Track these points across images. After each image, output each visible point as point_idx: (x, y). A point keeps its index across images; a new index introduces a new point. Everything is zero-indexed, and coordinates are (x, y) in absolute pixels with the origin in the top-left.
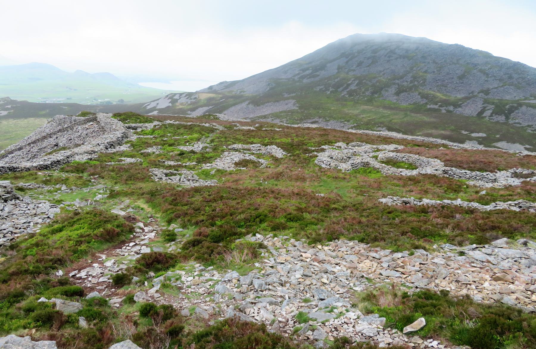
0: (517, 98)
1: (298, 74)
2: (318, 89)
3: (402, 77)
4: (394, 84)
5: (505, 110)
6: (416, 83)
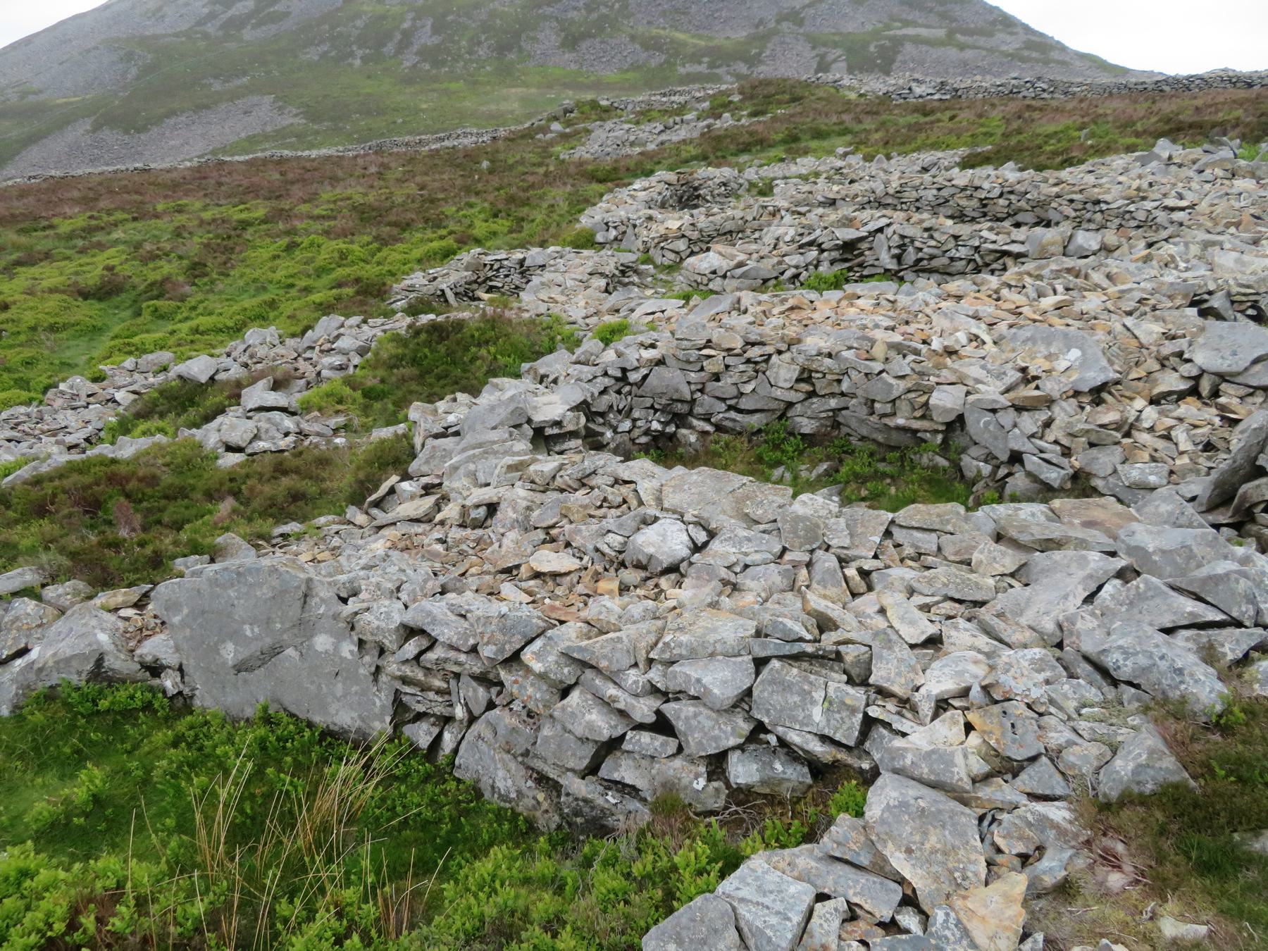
0: (869, 27)
1: (212, 16)
2: (312, 54)
4: (546, 18)
6: (604, 10)
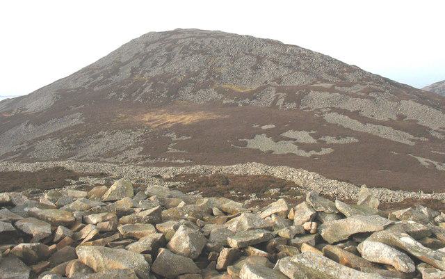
1: (89, 81)
3: (196, 74)
5: (296, 96)
6: (212, 78)
